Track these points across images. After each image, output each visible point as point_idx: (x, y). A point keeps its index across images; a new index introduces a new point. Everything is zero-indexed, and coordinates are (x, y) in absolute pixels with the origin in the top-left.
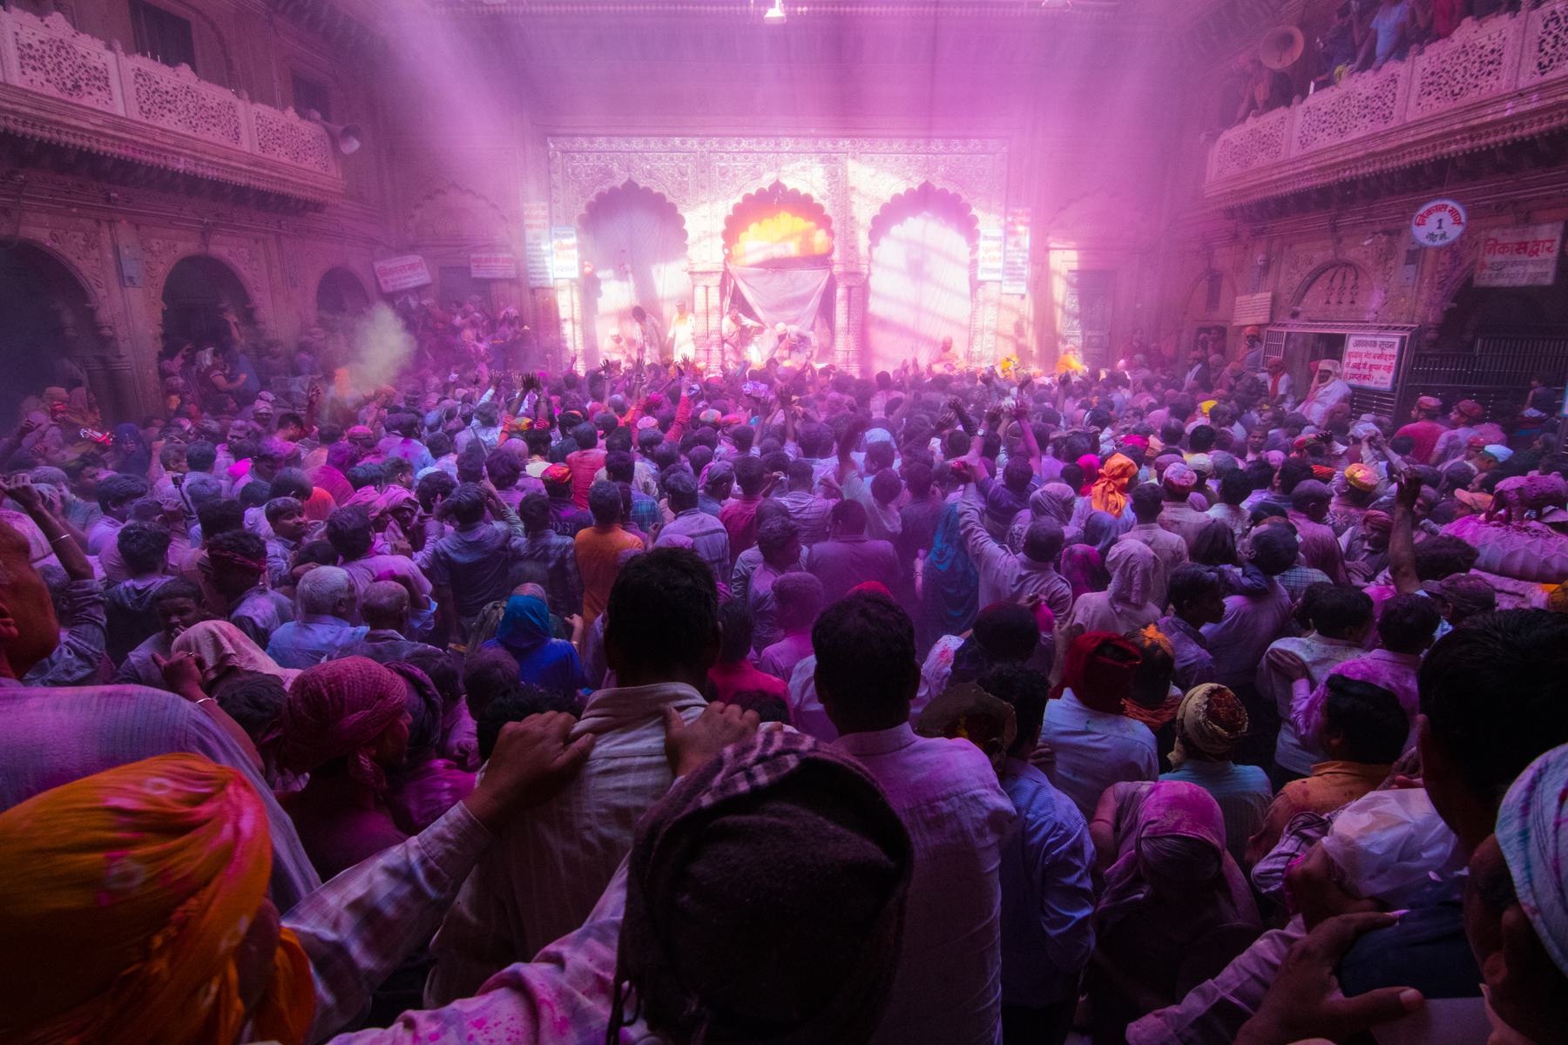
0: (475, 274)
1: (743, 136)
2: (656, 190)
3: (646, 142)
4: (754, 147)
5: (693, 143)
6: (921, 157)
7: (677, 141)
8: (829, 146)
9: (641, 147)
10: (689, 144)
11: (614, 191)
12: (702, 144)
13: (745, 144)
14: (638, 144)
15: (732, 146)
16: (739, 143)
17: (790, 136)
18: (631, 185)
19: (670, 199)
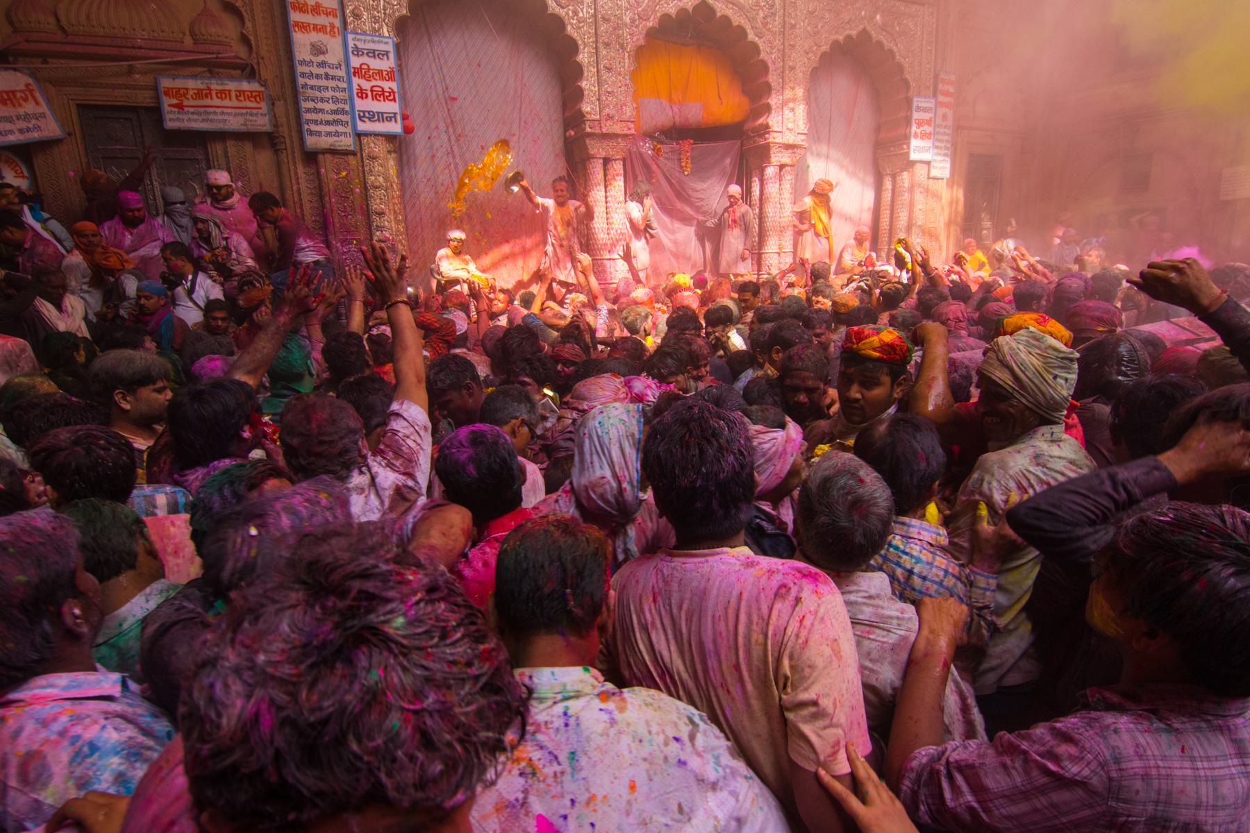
0: (173, 121)
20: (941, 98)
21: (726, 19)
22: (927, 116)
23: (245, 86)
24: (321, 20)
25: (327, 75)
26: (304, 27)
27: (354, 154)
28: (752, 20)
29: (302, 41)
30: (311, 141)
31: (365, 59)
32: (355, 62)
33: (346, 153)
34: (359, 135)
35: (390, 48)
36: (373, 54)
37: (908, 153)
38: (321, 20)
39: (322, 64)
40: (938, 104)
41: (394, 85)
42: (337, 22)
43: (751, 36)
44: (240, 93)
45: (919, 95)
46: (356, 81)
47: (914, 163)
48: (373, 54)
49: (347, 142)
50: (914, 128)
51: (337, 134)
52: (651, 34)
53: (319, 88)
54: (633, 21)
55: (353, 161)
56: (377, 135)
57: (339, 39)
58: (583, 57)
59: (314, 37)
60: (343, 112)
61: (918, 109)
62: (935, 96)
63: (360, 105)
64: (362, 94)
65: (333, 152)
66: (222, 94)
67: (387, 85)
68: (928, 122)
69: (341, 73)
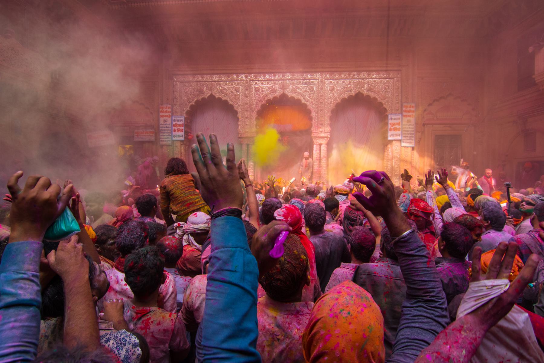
1: (267, 73)
2: (224, 99)
3: (220, 77)
4: (272, 78)
5: (242, 77)
6: (355, 81)
7: (235, 76)
8: (309, 76)
9: (217, 79)
10: (240, 78)
11: (203, 99)
12: (246, 77)
13: (267, 76)
14: (216, 78)
15: (261, 78)
16: (265, 76)
17: (290, 72)
18: (212, 96)
19: (231, 103)
20: (405, 114)
21: (293, 98)
22: (397, 121)
23: (151, 130)
24: (167, 114)
25: (167, 127)
26: (163, 116)
27: (171, 146)
28: (304, 96)
29: (162, 120)
30: (161, 143)
31: (176, 122)
32: (174, 123)
33: (169, 145)
34: (173, 141)
35: (183, 118)
36: (179, 121)
37: (387, 137)
38: (167, 114)
39: (165, 124)
40: (403, 116)
41: (183, 128)
42: (171, 114)
43: (303, 101)
44: (150, 132)
45: (392, 113)
46: (173, 128)
47: (391, 141)
48: (179, 121)
49: (170, 143)
50: (390, 126)
51: (168, 141)
52: (263, 106)
53: (164, 130)
54: (257, 103)
55: (171, 147)
56: (178, 141)
57: (170, 118)
58: (239, 115)
59: (165, 118)
60: (170, 135)
61: (391, 119)
62: (401, 113)
63: (174, 133)
64: (175, 131)
65: (167, 145)
66: (146, 132)
67: (181, 128)
68: (398, 124)
69: (170, 126)
